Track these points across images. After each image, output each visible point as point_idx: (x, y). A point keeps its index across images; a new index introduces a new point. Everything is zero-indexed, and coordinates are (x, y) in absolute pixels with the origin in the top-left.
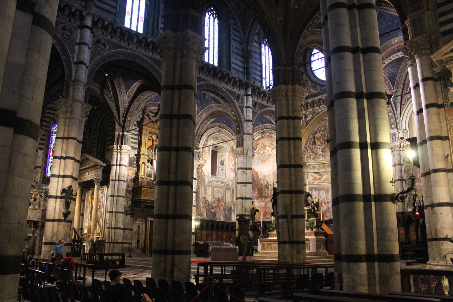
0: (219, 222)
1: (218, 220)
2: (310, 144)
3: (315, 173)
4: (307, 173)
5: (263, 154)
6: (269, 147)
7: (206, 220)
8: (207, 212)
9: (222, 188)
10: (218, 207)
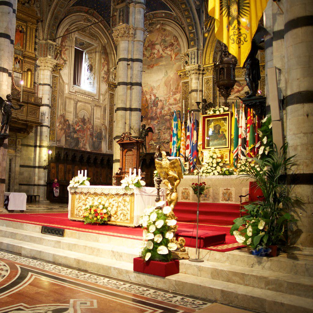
0: (84, 152)
1: (83, 149)
5: (150, 56)
6: (161, 46)
7: (65, 149)
8: (66, 137)
9: (90, 104)
10: (82, 130)
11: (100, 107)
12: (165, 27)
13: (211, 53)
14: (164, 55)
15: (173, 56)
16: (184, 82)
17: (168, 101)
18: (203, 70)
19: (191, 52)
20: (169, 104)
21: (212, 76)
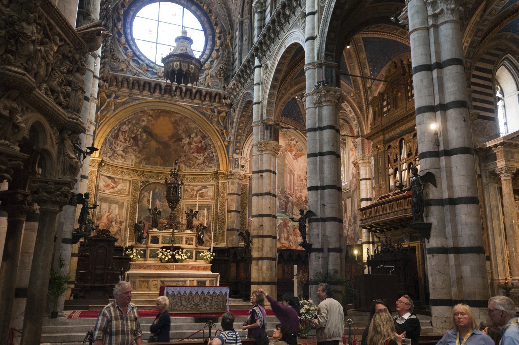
2: (112, 136)
3: (109, 177)
21: (97, 170)
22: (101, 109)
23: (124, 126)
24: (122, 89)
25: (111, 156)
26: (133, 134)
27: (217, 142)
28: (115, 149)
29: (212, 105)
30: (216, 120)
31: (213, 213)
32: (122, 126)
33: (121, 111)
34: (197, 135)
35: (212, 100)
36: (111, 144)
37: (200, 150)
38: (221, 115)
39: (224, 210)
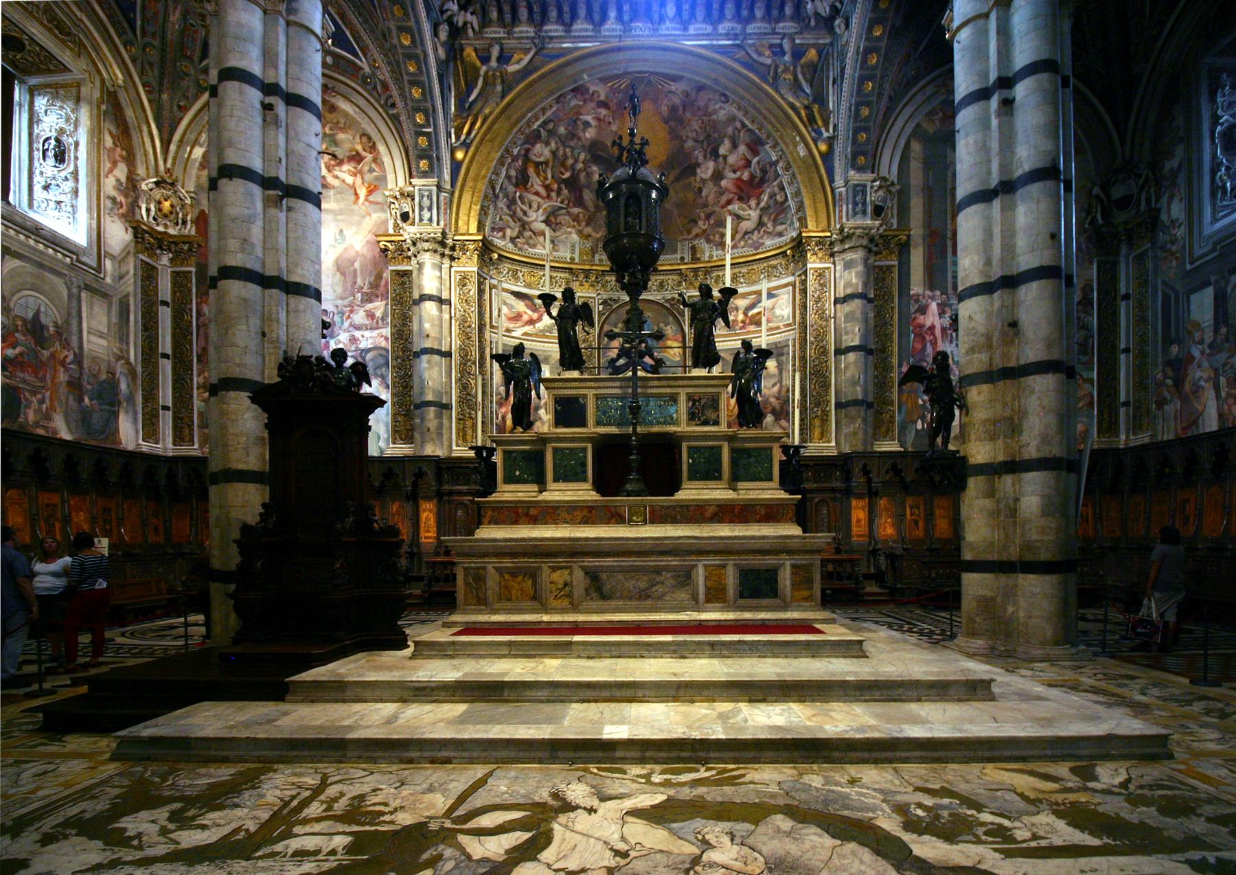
2: (508, 177)
4: (491, 289)
11: (105, 295)
12: (333, 100)
13: (473, 207)
14: (330, 180)
15: (362, 192)
16: (398, 273)
17: (349, 317)
18: (453, 249)
19: (419, 190)
20: (351, 325)
21: (476, 269)
22: (471, 99)
23: (538, 147)
24: (517, 29)
25: (518, 237)
26: (567, 170)
27: (796, 146)
28: (525, 218)
29: (774, 33)
30: (789, 77)
31: (794, 365)
32: (533, 145)
33: (519, 94)
34: (735, 146)
35: (775, 13)
36: (511, 203)
37: (747, 190)
38: (803, 60)
39: (824, 351)
